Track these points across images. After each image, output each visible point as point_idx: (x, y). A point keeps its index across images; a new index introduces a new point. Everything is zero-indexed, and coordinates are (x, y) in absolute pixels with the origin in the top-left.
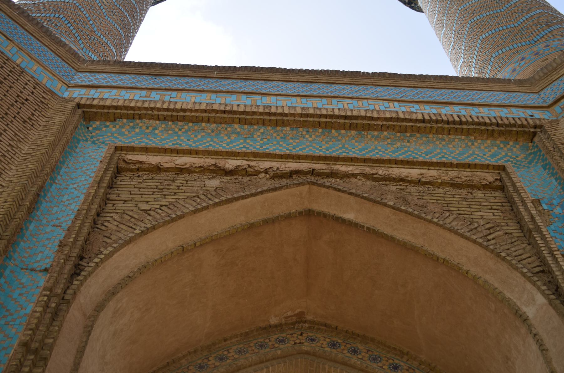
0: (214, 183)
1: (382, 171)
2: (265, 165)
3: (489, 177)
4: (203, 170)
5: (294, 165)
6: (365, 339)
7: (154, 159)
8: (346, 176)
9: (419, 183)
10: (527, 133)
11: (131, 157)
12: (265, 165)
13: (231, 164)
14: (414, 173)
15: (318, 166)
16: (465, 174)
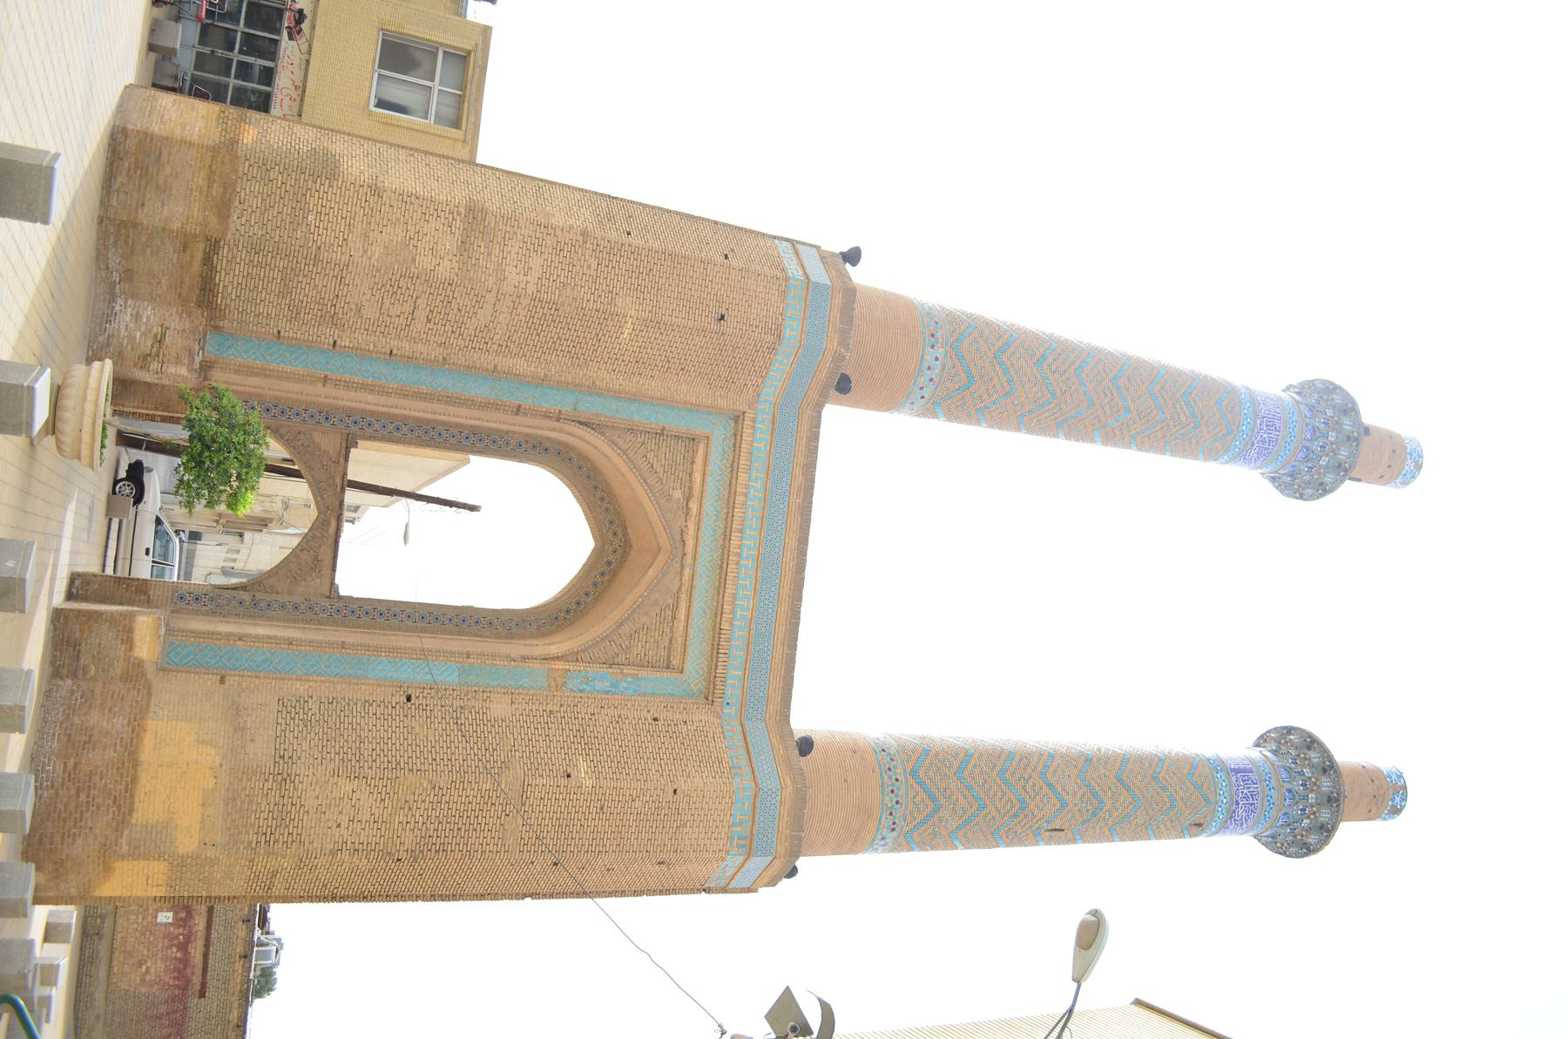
0: (678, 494)
1: (683, 596)
2: (691, 526)
3: (675, 662)
4: (691, 488)
5: (690, 543)
6: (610, 581)
7: (699, 459)
8: (681, 573)
9: (674, 618)
10: (710, 694)
11: (702, 447)
12: (691, 526)
13: (694, 506)
14: (682, 615)
15: (689, 560)
16: (678, 646)
